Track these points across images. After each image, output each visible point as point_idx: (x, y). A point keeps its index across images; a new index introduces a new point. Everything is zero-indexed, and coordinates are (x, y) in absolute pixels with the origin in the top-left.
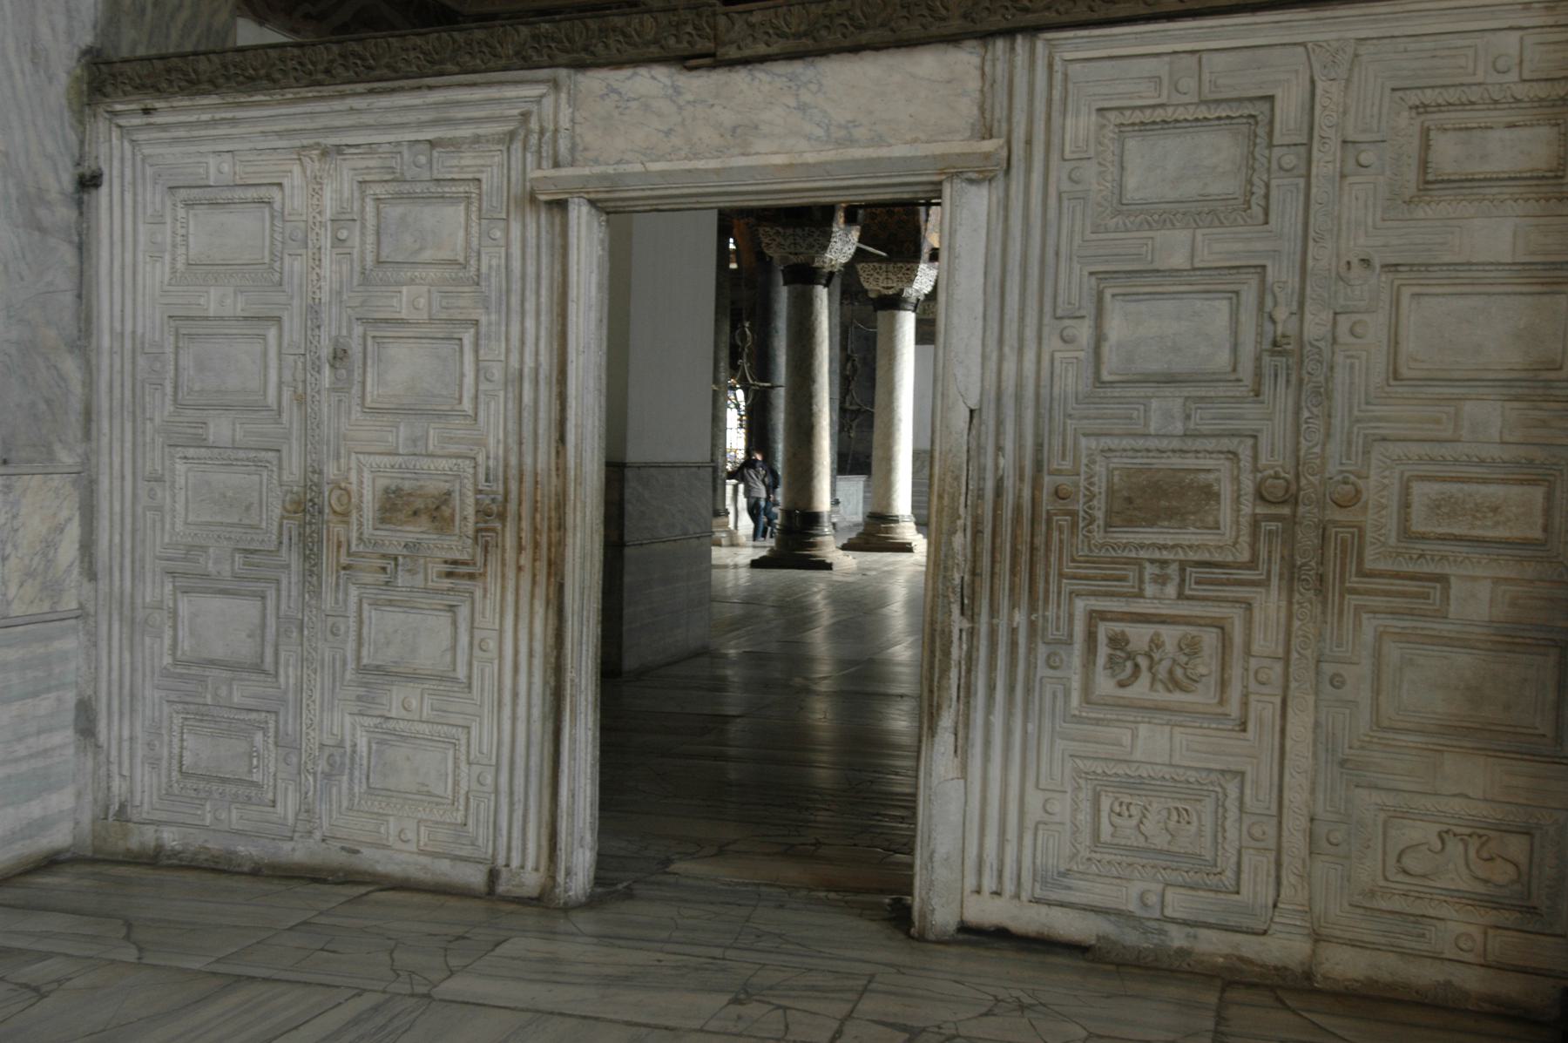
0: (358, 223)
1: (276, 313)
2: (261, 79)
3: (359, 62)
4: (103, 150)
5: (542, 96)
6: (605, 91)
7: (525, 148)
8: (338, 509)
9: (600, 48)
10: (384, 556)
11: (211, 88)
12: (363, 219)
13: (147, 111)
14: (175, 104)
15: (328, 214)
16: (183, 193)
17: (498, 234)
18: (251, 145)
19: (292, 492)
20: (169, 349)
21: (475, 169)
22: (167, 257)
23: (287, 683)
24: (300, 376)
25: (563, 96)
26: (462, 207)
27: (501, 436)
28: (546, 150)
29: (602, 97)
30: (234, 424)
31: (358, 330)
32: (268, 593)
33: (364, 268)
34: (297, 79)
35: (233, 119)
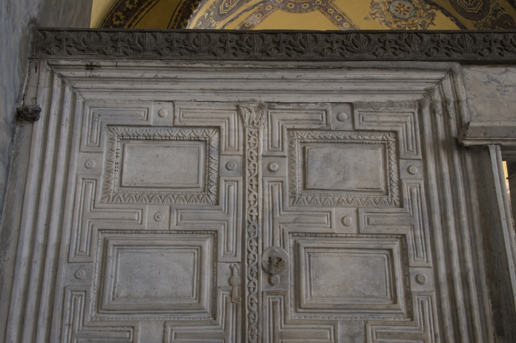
0: (287, 159)
1: (214, 228)
2: (204, 52)
3: (291, 48)
4: (44, 93)
5: (441, 80)
6: (487, 80)
7: (433, 112)
9: (486, 52)
11: (155, 55)
12: (292, 156)
13: (90, 67)
14: (119, 64)
15: (261, 152)
16: (120, 130)
17: (417, 169)
18: (192, 98)
20: (97, 258)
21: (392, 124)
22: (102, 181)
24: (237, 279)
25: (459, 80)
26: (380, 151)
27: (438, 331)
28: (452, 114)
29: (485, 83)
30: (165, 326)
31: (290, 242)
33: (294, 193)
34: (234, 54)
35: (176, 78)
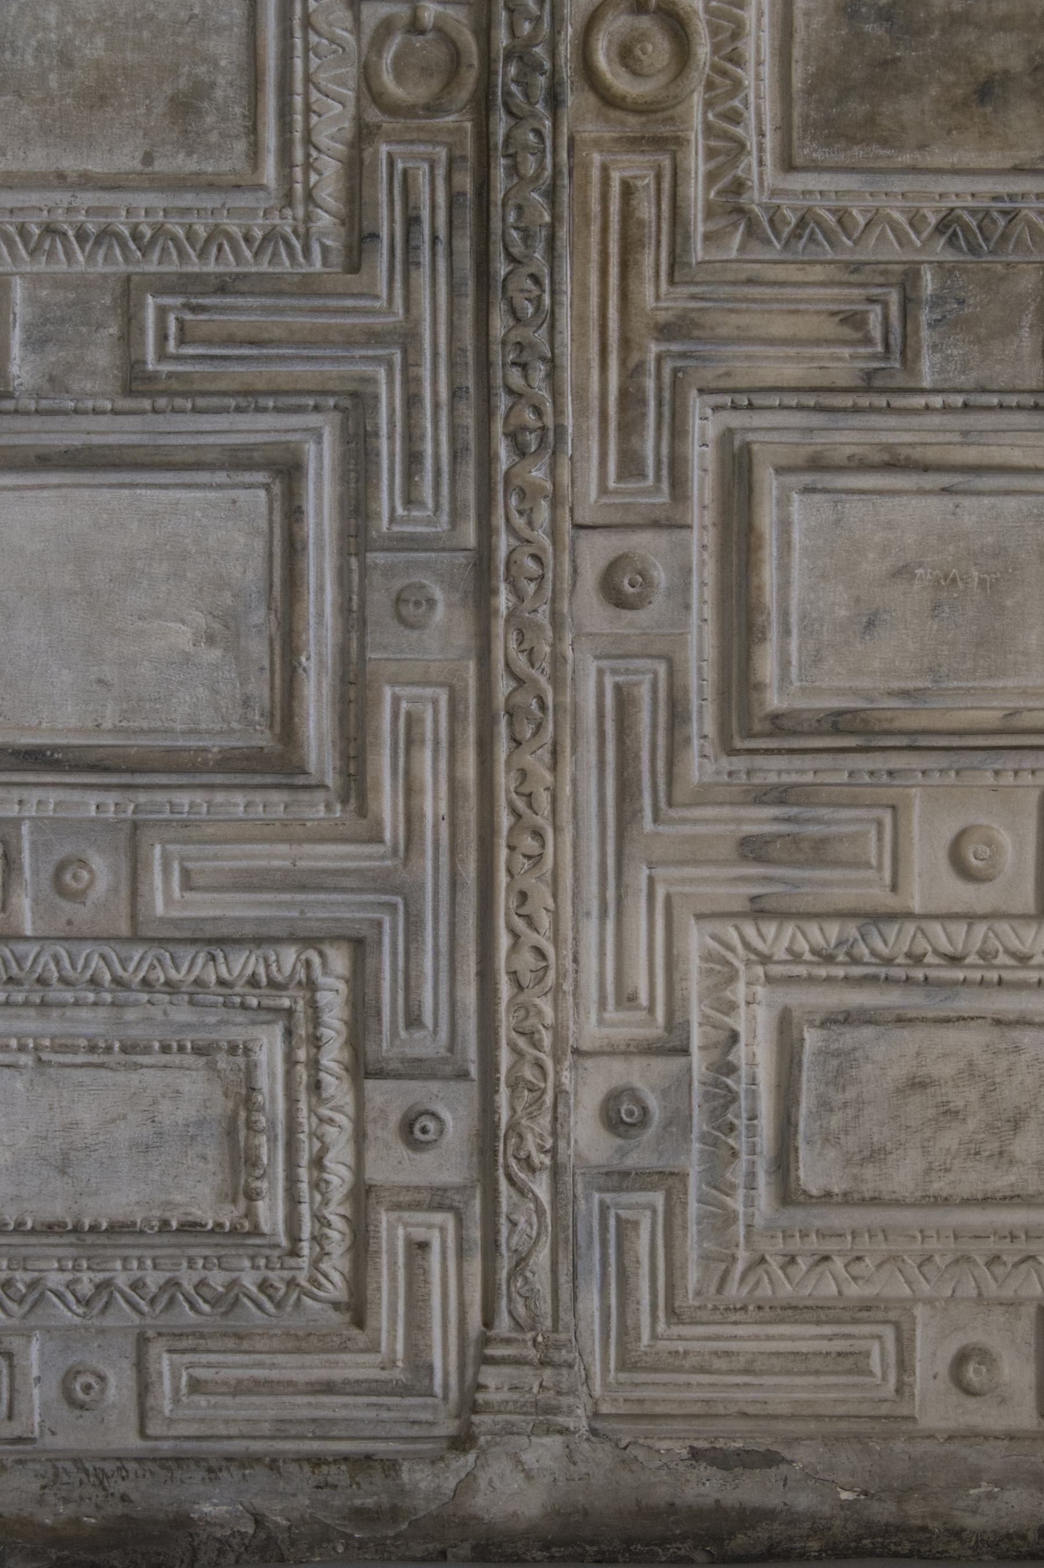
8: (621, 83)
10: (856, 267)
19: (415, 27)
23: (412, 818)
32: (311, 448)
